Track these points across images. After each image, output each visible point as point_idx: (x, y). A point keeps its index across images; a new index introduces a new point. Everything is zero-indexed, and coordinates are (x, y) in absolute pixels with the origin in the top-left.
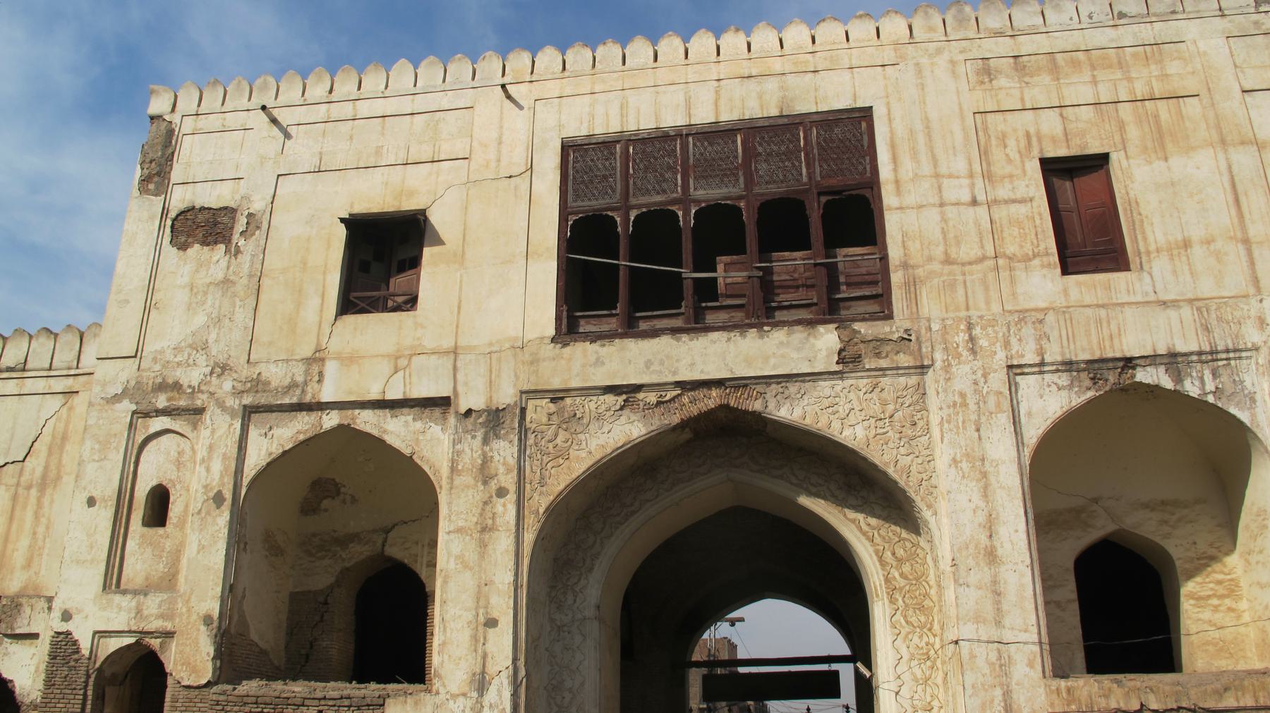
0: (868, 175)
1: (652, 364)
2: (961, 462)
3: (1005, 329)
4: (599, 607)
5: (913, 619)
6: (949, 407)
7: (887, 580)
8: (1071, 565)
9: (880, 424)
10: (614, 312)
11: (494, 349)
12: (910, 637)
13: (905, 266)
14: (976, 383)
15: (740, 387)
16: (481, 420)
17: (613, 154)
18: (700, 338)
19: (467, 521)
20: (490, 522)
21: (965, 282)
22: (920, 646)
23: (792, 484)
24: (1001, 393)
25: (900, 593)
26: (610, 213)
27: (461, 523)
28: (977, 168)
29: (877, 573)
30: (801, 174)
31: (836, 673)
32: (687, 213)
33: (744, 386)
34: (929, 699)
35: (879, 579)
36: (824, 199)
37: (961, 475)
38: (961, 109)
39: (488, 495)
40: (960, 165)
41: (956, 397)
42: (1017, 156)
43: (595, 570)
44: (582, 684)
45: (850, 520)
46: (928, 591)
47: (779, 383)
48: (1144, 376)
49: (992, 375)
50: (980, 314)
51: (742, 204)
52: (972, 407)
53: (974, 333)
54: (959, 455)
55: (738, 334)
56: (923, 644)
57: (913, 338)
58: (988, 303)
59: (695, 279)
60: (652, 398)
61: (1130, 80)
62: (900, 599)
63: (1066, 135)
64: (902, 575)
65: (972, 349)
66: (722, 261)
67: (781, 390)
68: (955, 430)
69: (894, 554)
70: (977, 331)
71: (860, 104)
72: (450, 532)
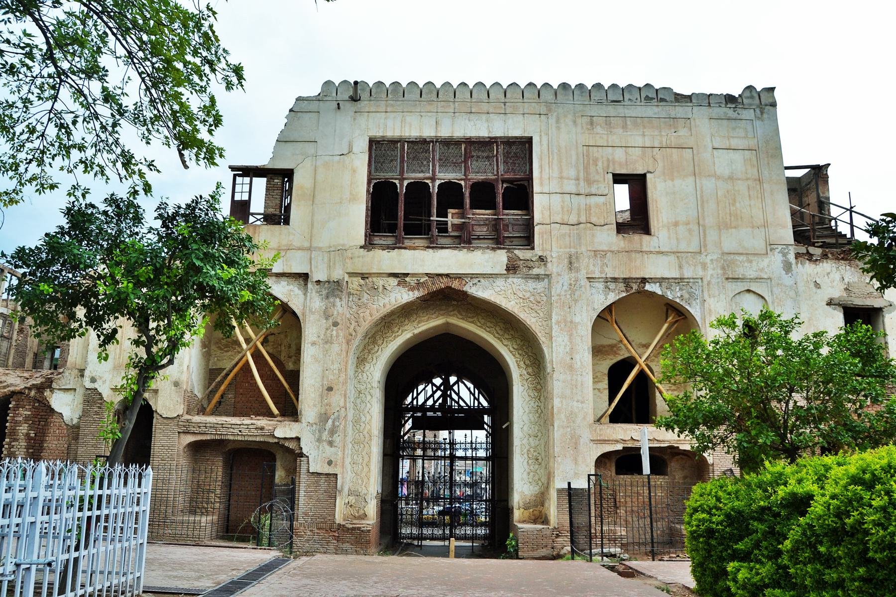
5: (532, 395)
7: (521, 375)
8: (606, 372)
9: (525, 301)
11: (332, 249)
26: (394, 181)
28: (582, 175)
36: (505, 185)
38: (577, 143)
40: (572, 173)
42: (602, 171)
44: (370, 420)
48: (648, 287)
51: (463, 183)
59: (437, 221)
61: (661, 136)
63: (627, 162)
66: (451, 211)
71: (526, 135)
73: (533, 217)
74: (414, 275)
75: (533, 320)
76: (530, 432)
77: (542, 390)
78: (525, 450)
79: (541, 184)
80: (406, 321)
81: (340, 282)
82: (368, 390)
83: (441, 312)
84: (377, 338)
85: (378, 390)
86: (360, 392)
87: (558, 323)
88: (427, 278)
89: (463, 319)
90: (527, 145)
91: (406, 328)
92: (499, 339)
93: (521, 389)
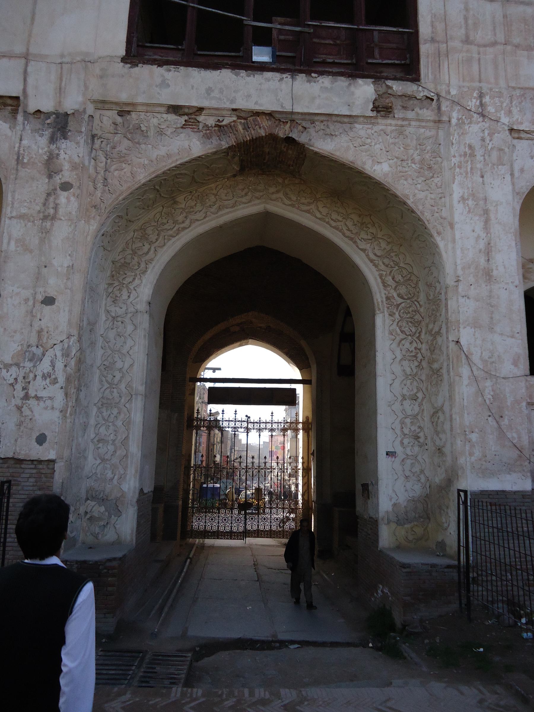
1: (213, 91)
2: (468, 199)
3: (507, 101)
4: (150, 303)
5: (406, 329)
6: (460, 156)
7: (388, 298)
10: (180, 47)
11: (65, 60)
12: (403, 342)
13: (433, 40)
14: (483, 140)
16: (48, 121)
18: (256, 75)
19: (29, 208)
20: (52, 211)
21: (479, 60)
22: (411, 350)
24: (502, 150)
25: (397, 309)
27: (24, 211)
29: (380, 292)
31: (294, 390)
34: (415, 390)
35: (382, 297)
37: (467, 210)
39: (51, 188)
41: (467, 149)
43: (149, 271)
44: (132, 365)
46: (418, 309)
49: (496, 135)
50: (490, 86)
52: (479, 158)
53: (484, 101)
54: (466, 194)
55: (289, 77)
56: (412, 349)
58: (497, 78)
60: (211, 121)
62: (397, 313)
64: (399, 295)
67: (322, 127)
68: (464, 174)
69: (393, 279)
70: (487, 99)
72: (12, 217)
73: (417, 32)
76: (405, 392)
77: (423, 324)
83: (258, 194)
84: (149, 231)
85: (146, 317)
87: (463, 199)
89: (293, 206)
92: (351, 239)
93: (388, 321)
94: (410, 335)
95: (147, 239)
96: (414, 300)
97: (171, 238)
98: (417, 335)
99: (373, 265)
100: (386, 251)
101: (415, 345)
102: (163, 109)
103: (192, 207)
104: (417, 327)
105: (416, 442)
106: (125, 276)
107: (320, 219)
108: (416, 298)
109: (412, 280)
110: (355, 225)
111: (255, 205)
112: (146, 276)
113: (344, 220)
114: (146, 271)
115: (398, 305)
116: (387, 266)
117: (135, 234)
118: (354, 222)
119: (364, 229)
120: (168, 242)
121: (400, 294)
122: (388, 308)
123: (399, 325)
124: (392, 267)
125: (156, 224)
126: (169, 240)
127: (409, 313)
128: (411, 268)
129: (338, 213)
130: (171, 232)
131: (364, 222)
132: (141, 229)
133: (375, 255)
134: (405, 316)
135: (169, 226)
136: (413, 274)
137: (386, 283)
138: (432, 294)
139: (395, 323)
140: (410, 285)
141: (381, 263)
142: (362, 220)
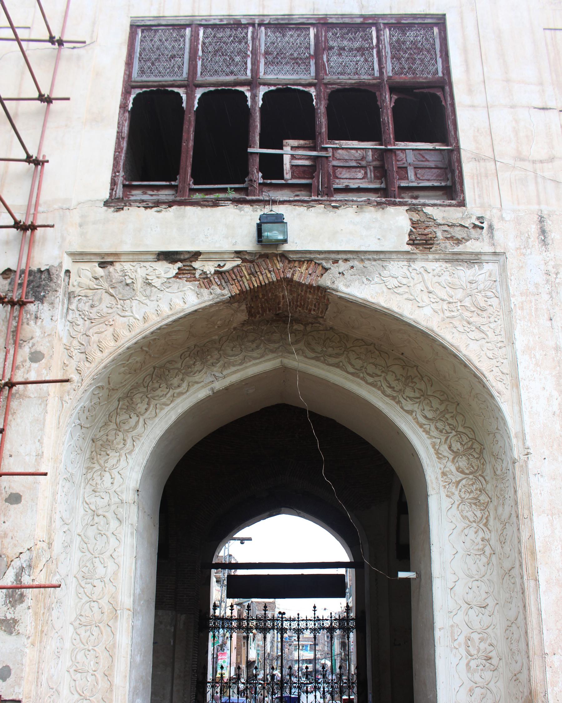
0: (440, 74)
4: (138, 491)
7: (444, 474)
10: (173, 183)
12: (466, 531)
15: (304, 262)
17: (183, 36)
22: (476, 541)
23: (348, 373)
25: (457, 487)
26: (176, 90)
30: (373, 69)
32: (254, 96)
33: (308, 261)
43: (137, 450)
44: (115, 573)
45: (407, 412)
46: (484, 486)
47: (346, 260)
51: (313, 91)
56: (479, 540)
57: (485, 225)
59: (261, 155)
60: (210, 268)
62: (457, 493)
64: (458, 469)
65: (543, 240)
69: (450, 448)
73: (458, 149)
74: (210, 256)
75: (474, 346)
76: (469, 598)
77: (491, 506)
78: (461, 639)
79: (470, 91)
80: (198, 363)
81: (53, 271)
82: (113, 507)
83: (272, 346)
84: (137, 398)
86: (95, 513)
88: (239, 262)
89: (317, 359)
90: (436, 30)
91: (197, 378)
92: (394, 398)
93: (446, 503)
94: (475, 522)
95: (134, 409)
96: (478, 474)
97: (164, 407)
98: (485, 521)
99: (423, 431)
100: (438, 412)
101: (481, 534)
102: (151, 257)
103: (189, 367)
104: (483, 510)
105: (488, 665)
106: (107, 457)
107: (352, 374)
108: (480, 473)
109: (475, 449)
110: (398, 380)
111: (269, 360)
112: (134, 456)
113: (383, 374)
114: (132, 451)
115: (458, 483)
116: (441, 432)
117: (121, 403)
118: (396, 376)
119: (410, 384)
120: (160, 412)
121: (459, 468)
122: (445, 487)
123: (460, 508)
124: (447, 433)
125: (145, 390)
126: (162, 409)
127: (472, 492)
128: (472, 433)
129: (376, 365)
130: (164, 400)
131: (409, 375)
132: (127, 397)
133: (426, 417)
134: (467, 495)
135: (162, 391)
136: (476, 440)
137: (441, 454)
138: (499, 468)
139: (455, 506)
140: (472, 455)
141: (433, 428)
142: (407, 374)
